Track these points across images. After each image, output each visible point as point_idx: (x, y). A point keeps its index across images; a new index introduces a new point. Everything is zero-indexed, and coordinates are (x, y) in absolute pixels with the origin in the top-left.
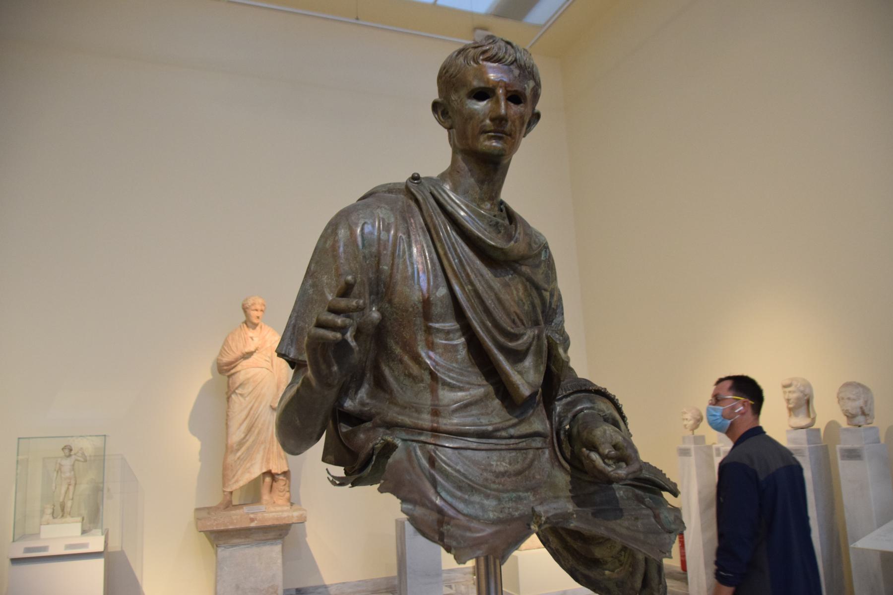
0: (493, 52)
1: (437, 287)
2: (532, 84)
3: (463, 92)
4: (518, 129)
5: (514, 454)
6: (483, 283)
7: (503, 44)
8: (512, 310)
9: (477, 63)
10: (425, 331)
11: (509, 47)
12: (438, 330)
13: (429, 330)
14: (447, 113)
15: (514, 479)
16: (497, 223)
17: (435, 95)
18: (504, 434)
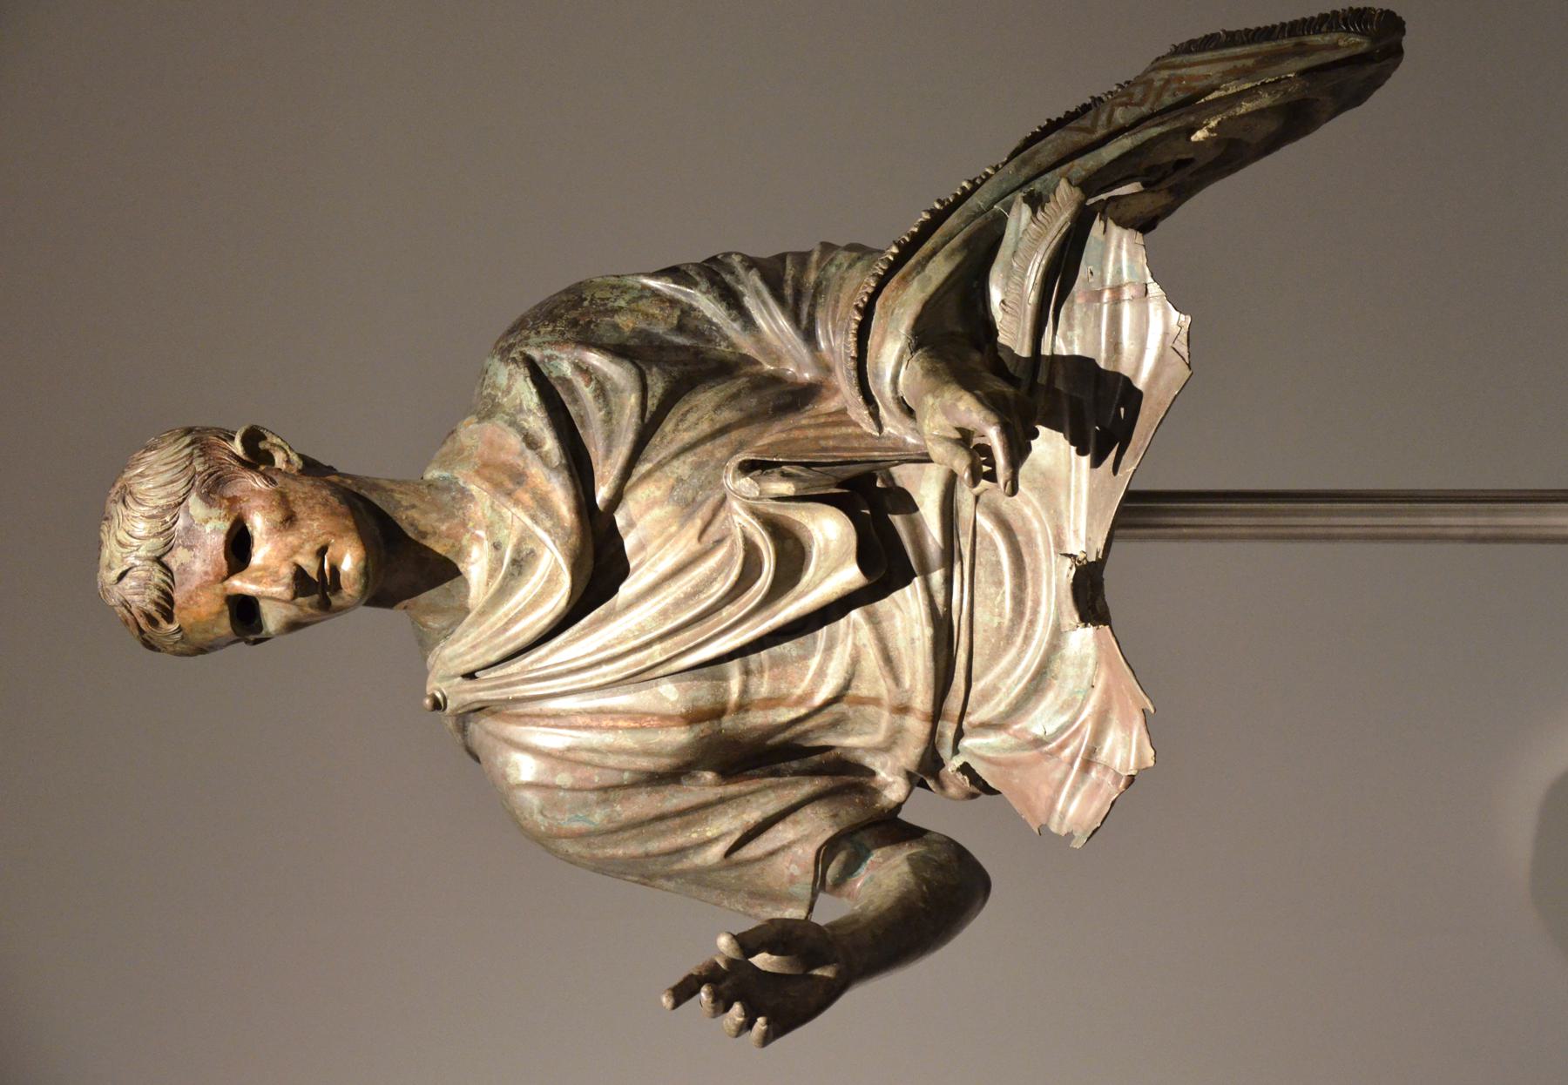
0: (151, 608)
1: (663, 699)
5: (980, 572)
8: (694, 546)
10: (747, 711)
12: (745, 691)
13: (742, 707)
15: (1029, 575)
18: (940, 599)
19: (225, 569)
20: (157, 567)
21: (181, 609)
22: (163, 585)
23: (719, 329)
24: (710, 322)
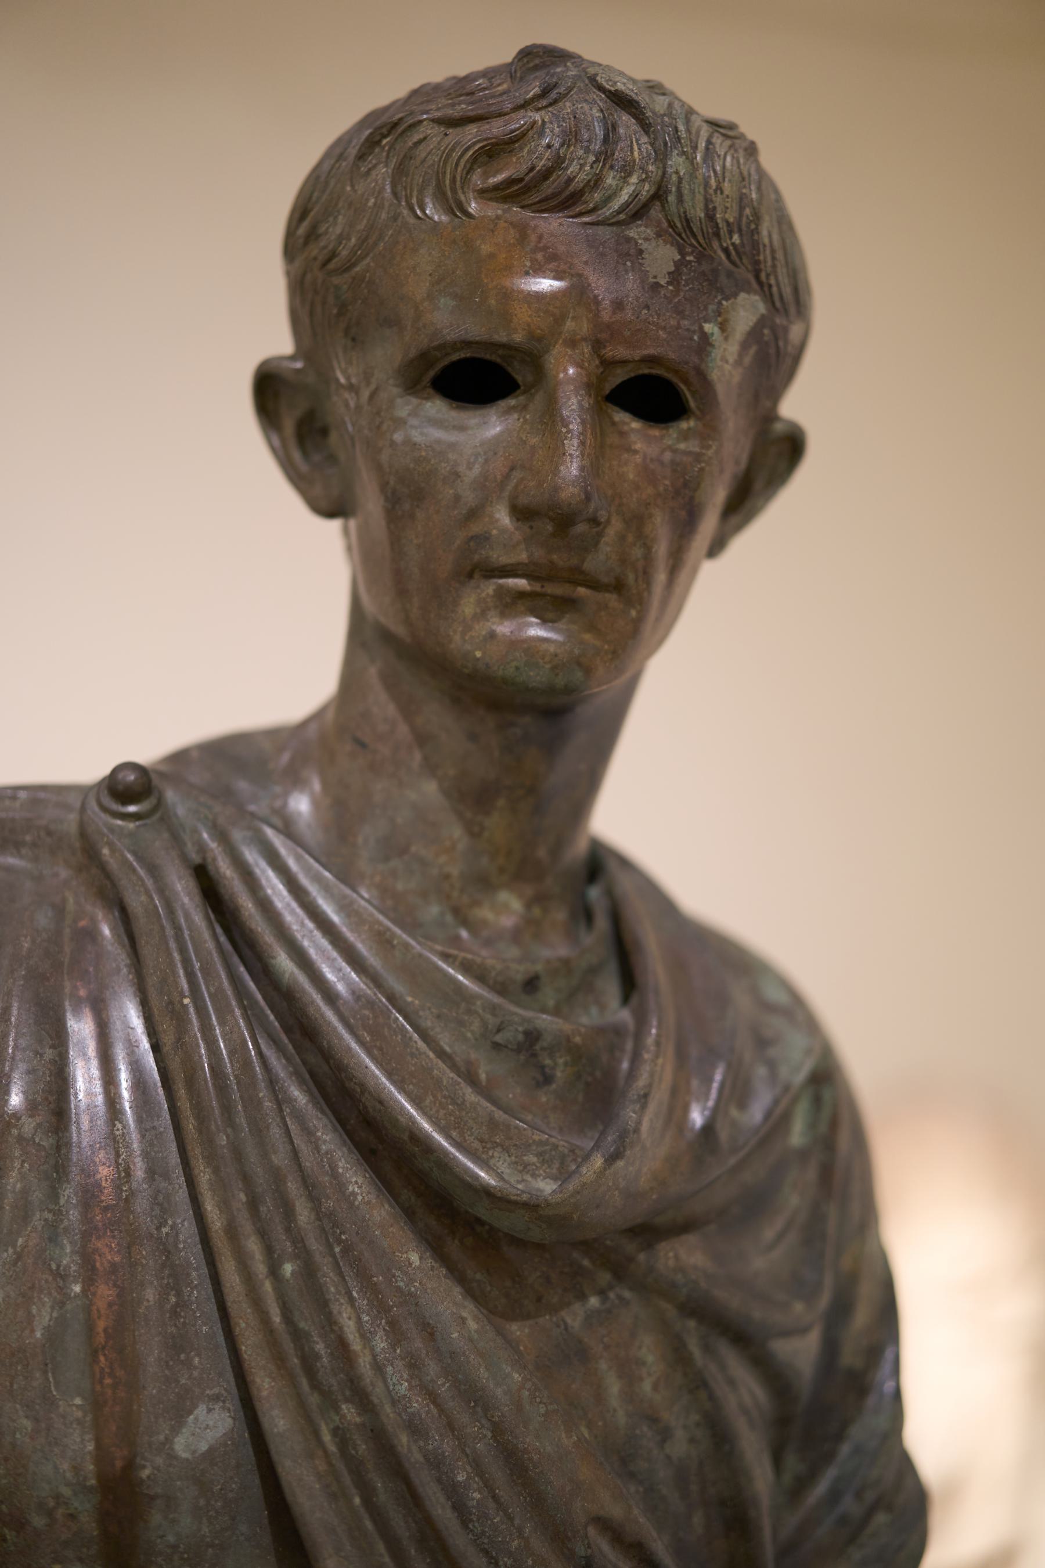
0: (537, 153)
1: (179, 1413)
2: (746, 311)
3: (386, 355)
4: (662, 549)
6: (432, 1368)
7: (593, 111)
9: (455, 208)
11: (626, 121)
14: (324, 432)
16: (532, 1037)
17: (272, 334)
19: (621, 352)
20: (647, 189)
21: (522, 230)
22: (597, 196)
23: (829, 1457)
24: (839, 1437)
